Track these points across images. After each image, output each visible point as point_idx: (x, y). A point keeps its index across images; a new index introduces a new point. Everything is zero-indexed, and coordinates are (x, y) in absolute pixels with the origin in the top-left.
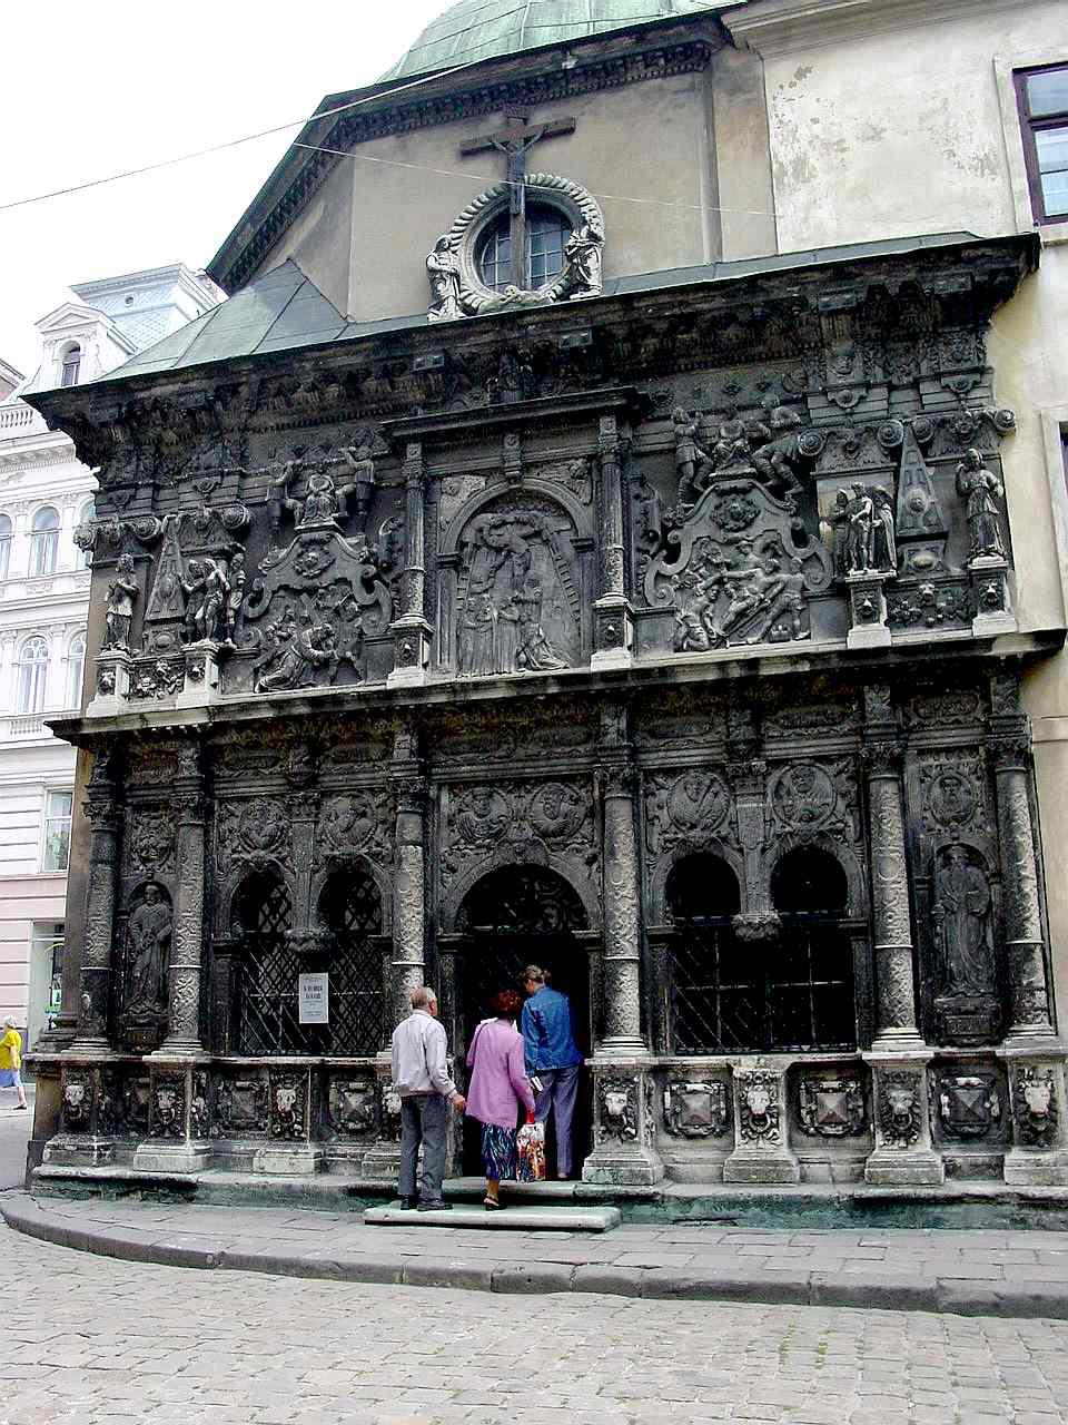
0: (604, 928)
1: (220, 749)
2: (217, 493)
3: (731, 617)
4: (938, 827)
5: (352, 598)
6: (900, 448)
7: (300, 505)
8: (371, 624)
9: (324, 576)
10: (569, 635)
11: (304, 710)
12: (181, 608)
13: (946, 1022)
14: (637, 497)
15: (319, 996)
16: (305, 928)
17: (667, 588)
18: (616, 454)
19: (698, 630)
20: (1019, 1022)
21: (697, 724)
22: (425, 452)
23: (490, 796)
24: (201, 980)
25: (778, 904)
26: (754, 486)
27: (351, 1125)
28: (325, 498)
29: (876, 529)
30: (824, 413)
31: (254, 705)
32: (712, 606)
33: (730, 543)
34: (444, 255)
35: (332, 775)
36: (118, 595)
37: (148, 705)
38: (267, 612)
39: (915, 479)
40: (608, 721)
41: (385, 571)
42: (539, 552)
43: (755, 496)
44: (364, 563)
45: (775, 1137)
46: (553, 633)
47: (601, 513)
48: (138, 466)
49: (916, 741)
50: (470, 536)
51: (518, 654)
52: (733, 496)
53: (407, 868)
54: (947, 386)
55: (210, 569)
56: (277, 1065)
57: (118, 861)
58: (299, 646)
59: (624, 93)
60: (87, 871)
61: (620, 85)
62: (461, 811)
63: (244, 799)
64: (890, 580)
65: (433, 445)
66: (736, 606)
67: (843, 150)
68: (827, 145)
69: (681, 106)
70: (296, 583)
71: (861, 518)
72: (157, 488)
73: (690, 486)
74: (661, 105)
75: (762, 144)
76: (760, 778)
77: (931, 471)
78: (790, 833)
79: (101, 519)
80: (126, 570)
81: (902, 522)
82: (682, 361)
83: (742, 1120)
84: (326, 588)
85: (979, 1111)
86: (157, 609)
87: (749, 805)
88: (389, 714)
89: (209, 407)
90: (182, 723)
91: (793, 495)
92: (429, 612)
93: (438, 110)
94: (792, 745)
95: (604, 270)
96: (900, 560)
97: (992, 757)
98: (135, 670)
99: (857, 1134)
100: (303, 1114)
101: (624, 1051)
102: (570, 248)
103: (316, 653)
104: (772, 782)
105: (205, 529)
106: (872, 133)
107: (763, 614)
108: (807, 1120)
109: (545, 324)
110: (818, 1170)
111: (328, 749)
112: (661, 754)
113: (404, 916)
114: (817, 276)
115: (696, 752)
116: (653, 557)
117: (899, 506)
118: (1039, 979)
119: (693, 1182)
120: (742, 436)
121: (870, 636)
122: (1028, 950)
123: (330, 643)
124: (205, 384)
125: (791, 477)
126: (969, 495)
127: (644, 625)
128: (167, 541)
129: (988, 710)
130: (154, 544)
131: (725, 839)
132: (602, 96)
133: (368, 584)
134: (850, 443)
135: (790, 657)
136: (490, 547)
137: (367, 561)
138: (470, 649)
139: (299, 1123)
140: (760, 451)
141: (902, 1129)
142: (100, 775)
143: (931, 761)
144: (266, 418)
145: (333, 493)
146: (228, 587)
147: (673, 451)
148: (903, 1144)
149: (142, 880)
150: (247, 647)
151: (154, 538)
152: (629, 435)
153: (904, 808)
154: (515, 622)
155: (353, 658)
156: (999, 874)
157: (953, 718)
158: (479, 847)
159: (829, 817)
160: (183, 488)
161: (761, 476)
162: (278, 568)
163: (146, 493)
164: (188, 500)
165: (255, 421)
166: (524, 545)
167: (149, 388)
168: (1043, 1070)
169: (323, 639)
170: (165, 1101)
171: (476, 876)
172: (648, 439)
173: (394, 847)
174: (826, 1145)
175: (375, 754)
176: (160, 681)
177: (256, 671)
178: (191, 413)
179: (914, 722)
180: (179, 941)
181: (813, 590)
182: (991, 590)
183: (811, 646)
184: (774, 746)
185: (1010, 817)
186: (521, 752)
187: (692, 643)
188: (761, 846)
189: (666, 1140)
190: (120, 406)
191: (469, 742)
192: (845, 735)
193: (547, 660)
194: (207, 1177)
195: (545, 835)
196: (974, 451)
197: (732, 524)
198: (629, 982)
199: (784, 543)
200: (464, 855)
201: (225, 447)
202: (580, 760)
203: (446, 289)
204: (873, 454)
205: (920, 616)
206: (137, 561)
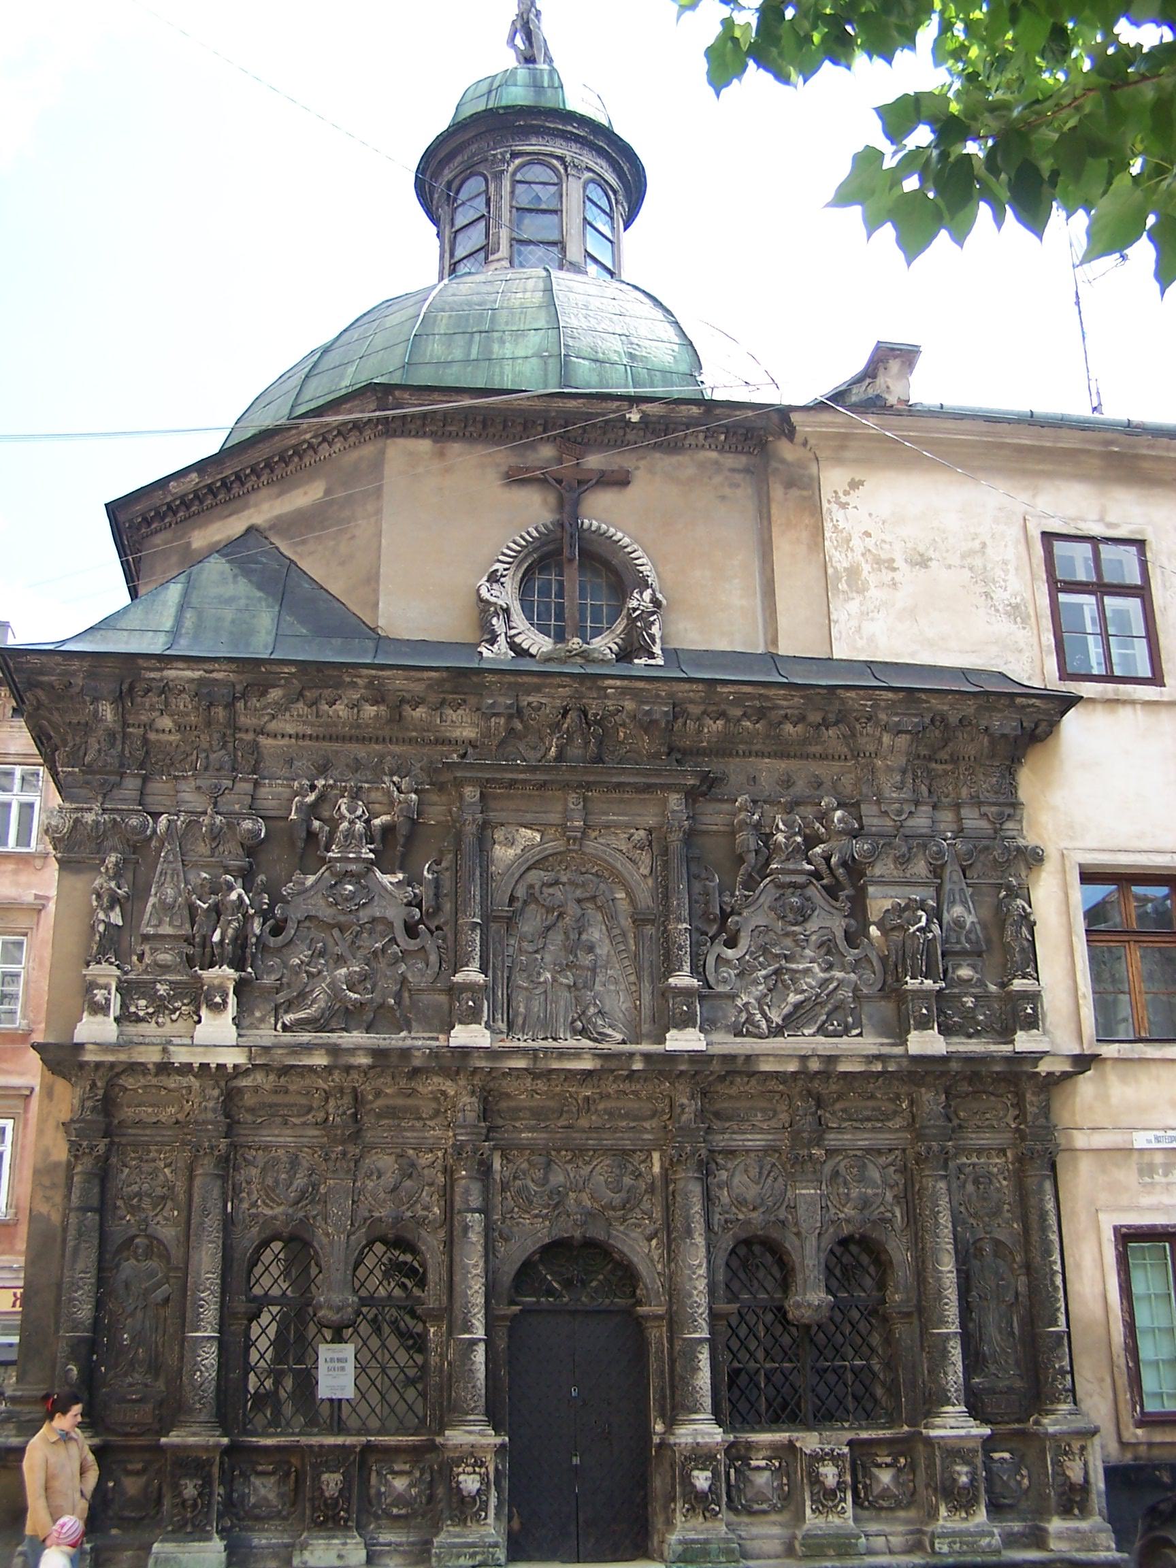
1: (240, 1091)
2: (228, 797)
4: (972, 1221)
5: (393, 940)
6: (943, 866)
7: (327, 828)
8: (417, 973)
9: (361, 914)
11: (364, 1060)
12: (188, 926)
13: (982, 1402)
14: (697, 877)
15: (343, 1369)
17: (729, 973)
20: (1052, 1403)
21: (763, 1110)
23: (549, 1164)
24: (221, 1348)
25: (829, 1291)
27: (395, 1511)
28: (359, 826)
30: (875, 821)
31: (308, 1048)
33: (787, 934)
34: (495, 586)
36: (114, 901)
37: (149, 1029)
39: (957, 897)
40: (685, 1101)
44: (409, 904)
45: (844, 1511)
46: (607, 1002)
48: (123, 750)
50: (521, 892)
51: (573, 1021)
52: (791, 890)
54: (985, 814)
55: (231, 888)
56: (321, 1446)
57: (103, 1208)
58: (333, 985)
59: (680, 458)
60: (56, 1218)
61: (674, 448)
62: (515, 1178)
63: (266, 1148)
66: (793, 998)
67: (894, 569)
68: (878, 561)
69: (738, 486)
71: (918, 930)
73: (750, 875)
74: (718, 479)
75: (816, 544)
76: (818, 1167)
78: (848, 1221)
79: (74, 806)
80: (117, 875)
82: (742, 747)
83: (812, 1494)
85: (1012, 1483)
90: (213, 1060)
91: (847, 897)
92: (483, 970)
93: (485, 426)
94: (849, 1137)
95: (662, 638)
96: (945, 971)
98: (126, 990)
99: (907, 1507)
100: (349, 1500)
102: (635, 610)
104: (827, 1169)
106: (919, 559)
107: (818, 1008)
108: (862, 1495)
109: (623, 691)
110: (879, 1542)
111: (372, 1102)
112: (726, 1136)
113: (471, 1288)
114: (890, 695)
115: (759, 1137)
116: (713, 939)
117: (944, 922)
118: (1066, 1363)
119: (758, 1557)
120: (799, 833)
121: (926, 1042)
122: (1059, 1336)
127: (707, 1004)
129: (1021, 1116)
131: (783, 1222)
132: (658, 455)
133: (411, 930)
134: (904, 856)
135: (867, 1057)
137: (409, 904)
138: (522, 1010)
139: (347, 1511)
140: (818, 850)
141: (962, 1501)
142: (94, 1109)
143: (965, 1160)
145: (368, 822)
146: (251, 911)
147: (733, 834)
148: (964, 1515)
149: (134, 1231)
150: (268, 980)
154: (569, 987)
156: (1028, 1267)
157: (987, 1123)
158: (536, 1216)
159: (878, 1207)
160: (183, 786)
162: (304, 896)
163: (131, 784)
165: (273, 726)
167: (161, 670)
174: (877, 1519)
175: (427, 1109)
176: (161, 1006)
179: (956, 1122)
180: (202, 1306)
182: (1029, 1011)
184: (832, 1136)
185: (1043, 1216)
186: (583, 1122)
187: (751, 1029)
188: (817, 1231)
191: (530, 1109)
192: (897, 1130)
193: (609, 1031)
200: (518, 1224)
202: (646, 1136)
203: (498, 624)
204: (920, 868)
205: (961, 1026)
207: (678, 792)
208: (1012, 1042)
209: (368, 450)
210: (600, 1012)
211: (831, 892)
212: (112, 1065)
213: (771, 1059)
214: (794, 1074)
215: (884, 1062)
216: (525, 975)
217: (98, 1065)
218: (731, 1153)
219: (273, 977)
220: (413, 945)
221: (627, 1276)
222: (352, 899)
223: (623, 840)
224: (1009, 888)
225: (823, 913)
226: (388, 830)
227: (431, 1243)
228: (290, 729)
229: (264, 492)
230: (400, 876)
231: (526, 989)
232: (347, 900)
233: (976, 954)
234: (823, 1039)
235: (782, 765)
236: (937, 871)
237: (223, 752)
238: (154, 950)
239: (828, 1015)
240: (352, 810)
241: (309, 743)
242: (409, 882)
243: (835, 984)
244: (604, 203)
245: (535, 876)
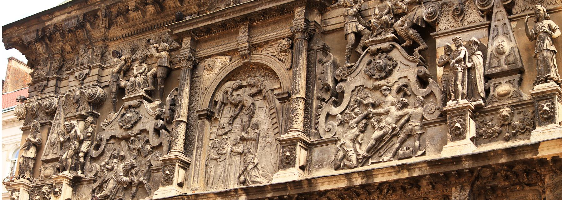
3: (372, 142)
5: (147, 142)
10: (273, 162)
14: (320, 61)
18: (303, 32)
19: (350, 153)
22: (195, 43)
26: (394, 47)
28: (140, 79)
29: (469, 69)
32: (362, 135)
33: (376, 88)
38: (103, 153)
39: (500, 31)
41: (167, 121)
42: (259, 103)
44: (158, 117)
50: (219, 97)
51: (240, 176)
52: (379, 55)
64: (478, 108)
65: (199, 36)
66: (378, 134)
71: (459, 62)
72: (59, 79)
77: (514, 24)
81: (490, 63)
84: (135, 136)
86: (48, 153)
89: (81, 26)
91: (420, 52)
92: (187, 149)
96: (487, 91)
103: (126, 179)
105: (77, 102)
107: (395, 139)
116: (326, 102)
117: (489, 52)
120: (388, 13)
123: (133, 172)
124: (78, 13)
125: (419, 39)
126: (536, 39)
128: (57, 112)
130: (51, 113)
136: (231, 103)
137: (158, 117)
138: (212, 173)
140: (399, 22)
144: (116, 31)
146: (82, 137)
150: (90, 176)
151: (53, 109)
152: (318, 19)
154: (240, 154)
155: (145, 182)
160: (72, 78)
161: (399, 40)
163: (52, 83)
164: (71, 86)
166: (250, 101)
167: (51, 19)
169: (130, 169)
172: (333, 21)
177: (94, 191)
178: (70, 31)
181: (428, 118)
182: (546, 108)
187: (348, 163)
190: (38, 31)
193: (258, 180)
196: (539, 7)
197: (377, 76)
199: (412, 85)
201: (93, 52)
205: (500, 133)
206: (42, 125)
207: (301, 6)
208: (529, 138)
210: (255, 166)
211: (410, 50)
213: (325, 180)
214: (346, 189)
215: (409, 170)
216: (217, 149)
219: (93, 174)
222: (129, 121)
225: (403, 67)
226: (154, 76)
230: (158, 102)
231: (216, 159)
232: (127, 123)
233: (516, 72)
237: (85, 54)
238: (46, 168)
239: (402, 143)
240: (137, 70)
241: (129, 38)
242: (161, 106)
243: (406, 118)
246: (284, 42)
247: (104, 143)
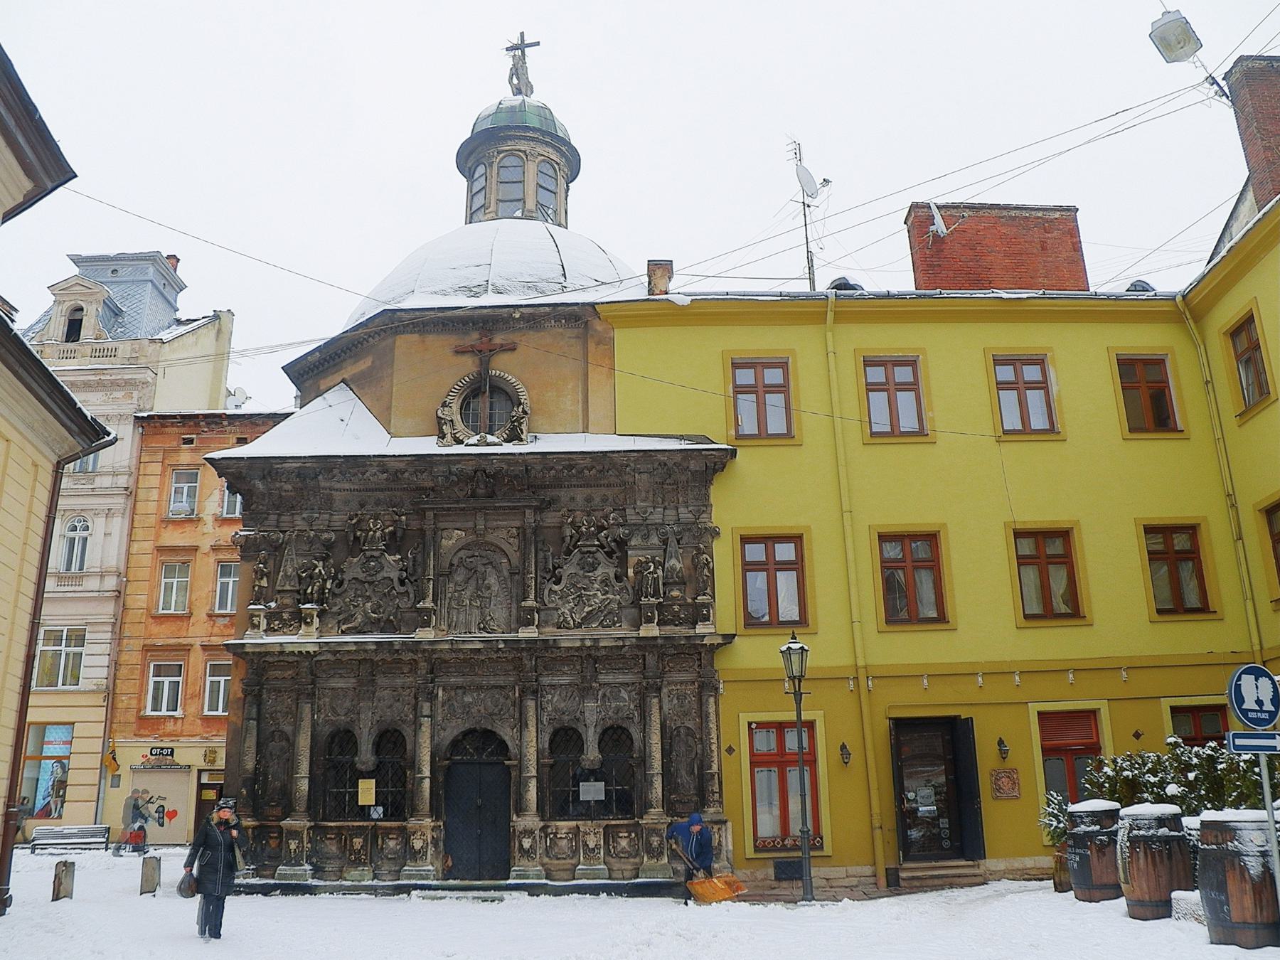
0: (520, 761)
8: (405, 603)
11: (374, 647)
16: (366, 756)
25: (600, 752)
28: (378, 534)
35: (381, 680)
41: (412, 577)
43: (598, 555)
47: (524, 559)
49: (668, 678)
50: (455, 562)
53: (423, 729)
57: (259, 719)
60: (239, 723)
66: (587, 609)
70: (361, 576)
72: (279, 515)
87: (590, 704)
88: (415, 652)
90: (304, 650)
92: (435, 600)
97: (701, 686)
98: (271, 616)
101: (529, 821)
121: (651, 631)
122: (713, 775)
130: (277, 548)
141: (655, 853)
149: (273, 728)
150: (335, 609)
153: (661, 708)
160: (296, 517)
161: (602, 546)
165: (338, 486)
168: (716, 828)
170: (293, 845)
171: (456, 733)
173: (416, 717)
176: (285, 624)
183: (621, 634)
185: (707, 716)
189: (546, 860)
194: (315, 882)
195: (491, 714)
198: (533, 785)
203: (446, 429)
209: (390, 341)
211: (610, 554)
212: (260, 653)
217: (253, 653)
218: (553, 686)
220: (402, 589)
221: (503, 747)
223: (503, 533)
224: (698, 549)
226: (393, 534)
227: (407, 731)
228: (347, 486)
229: (349, 361)
233: (682, 583)
234: (601, 631)
235: (588, 491)
236: (665, 542)
242: (401, 560)
244: (551, 172)
245: (462, 554)
246: (514, 531)
247: (346, 583)
